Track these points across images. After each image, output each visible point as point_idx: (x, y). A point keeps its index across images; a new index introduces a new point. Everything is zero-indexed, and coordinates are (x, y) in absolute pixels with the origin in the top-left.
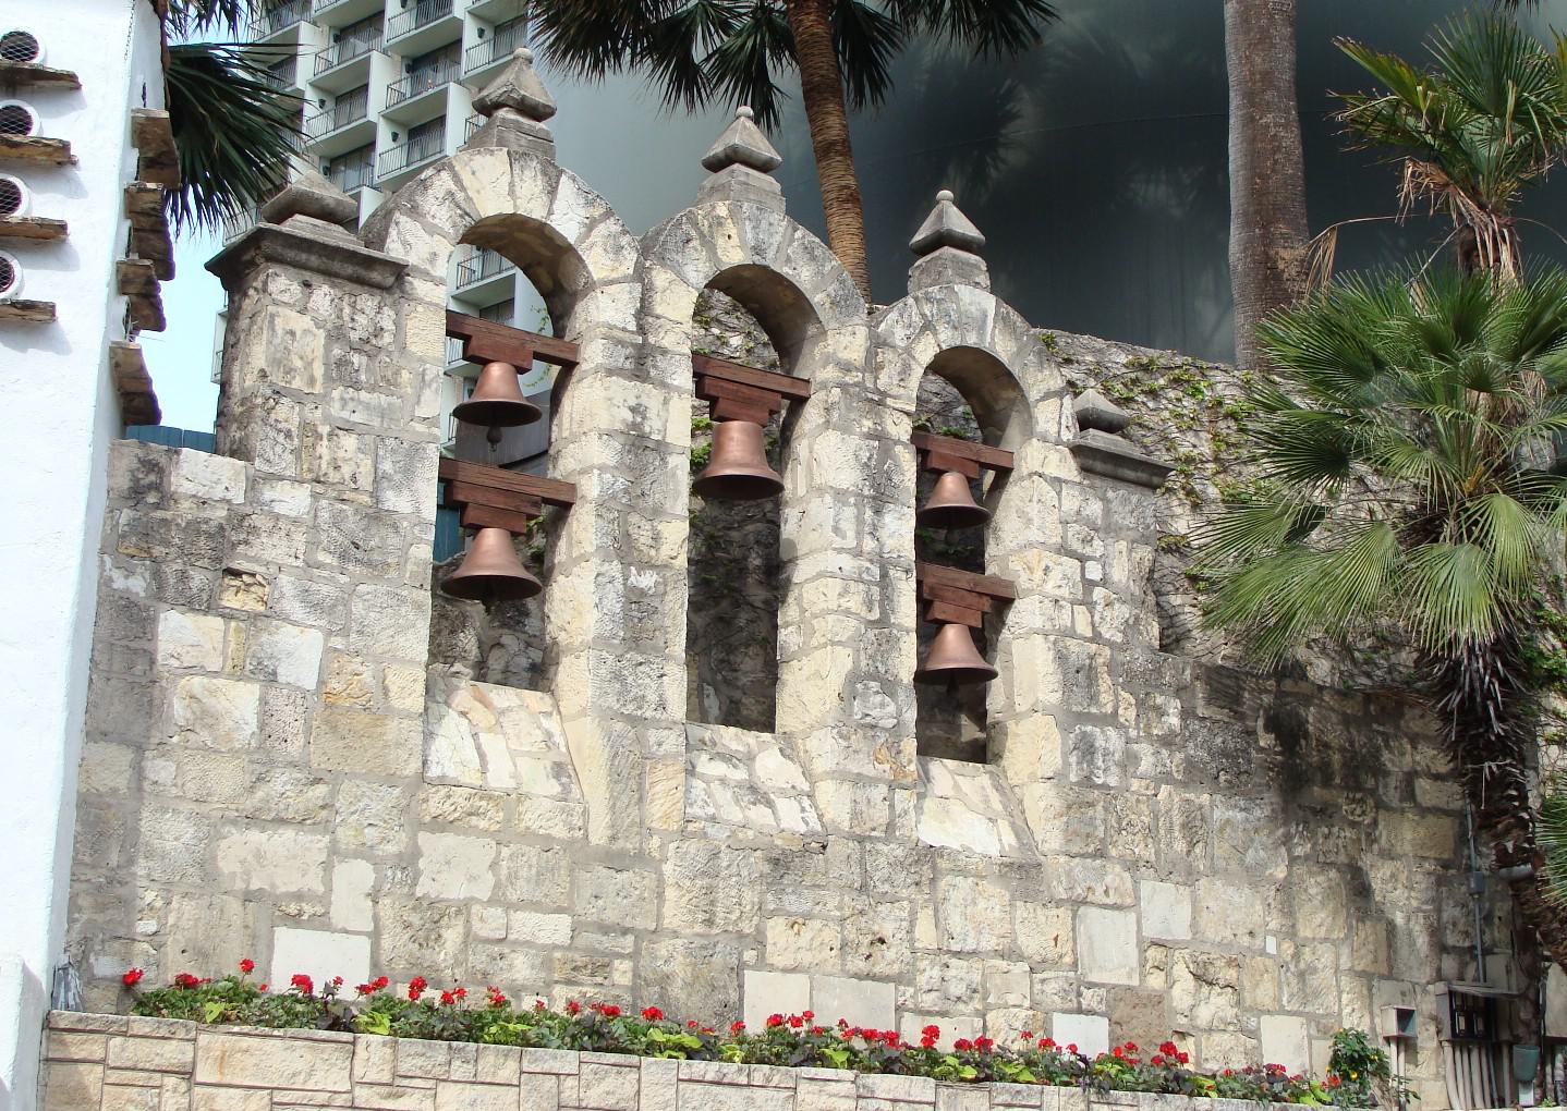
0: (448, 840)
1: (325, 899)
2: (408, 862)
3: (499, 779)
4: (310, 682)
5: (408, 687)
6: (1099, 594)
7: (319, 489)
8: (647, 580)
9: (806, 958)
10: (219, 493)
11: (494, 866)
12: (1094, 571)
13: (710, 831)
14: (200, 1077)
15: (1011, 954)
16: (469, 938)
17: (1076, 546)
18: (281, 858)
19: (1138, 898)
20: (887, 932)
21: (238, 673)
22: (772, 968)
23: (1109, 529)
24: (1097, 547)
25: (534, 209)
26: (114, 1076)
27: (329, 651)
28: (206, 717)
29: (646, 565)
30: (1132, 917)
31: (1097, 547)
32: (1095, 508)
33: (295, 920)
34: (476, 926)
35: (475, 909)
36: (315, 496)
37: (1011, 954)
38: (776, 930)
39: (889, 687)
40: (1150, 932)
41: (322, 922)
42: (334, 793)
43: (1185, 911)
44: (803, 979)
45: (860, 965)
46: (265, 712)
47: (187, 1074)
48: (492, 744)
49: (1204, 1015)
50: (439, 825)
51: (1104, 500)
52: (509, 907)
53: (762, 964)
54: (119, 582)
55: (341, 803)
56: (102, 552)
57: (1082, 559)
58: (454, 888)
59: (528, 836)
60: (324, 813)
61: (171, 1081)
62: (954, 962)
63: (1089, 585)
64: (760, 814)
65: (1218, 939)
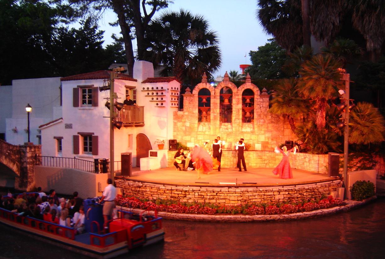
1: (191, 140)
2: (197, 137)
5: (196, 125)
6: (262, 108)
8: (216, 114)
12: (261, 106)
15: (251, 139)
16: (202, 142)
17: (259, 104)
18: (187, 138)
23: (263, 102)
24: (262, 104)
25: (205, 87)
29: (215, 113)
31: (262, 104)
32: (261, 100)
33: (189, 142)
37: (251, 139)
39: (239, 119)
41: (190, 142)
46: (186, 128)
49: (272, 143)
51: (263, 99)
54: (175, 121)
57: (260, 105)
58: (200, 139)
59: (206, 135)
63: (261, 107)
64: (227, 131)
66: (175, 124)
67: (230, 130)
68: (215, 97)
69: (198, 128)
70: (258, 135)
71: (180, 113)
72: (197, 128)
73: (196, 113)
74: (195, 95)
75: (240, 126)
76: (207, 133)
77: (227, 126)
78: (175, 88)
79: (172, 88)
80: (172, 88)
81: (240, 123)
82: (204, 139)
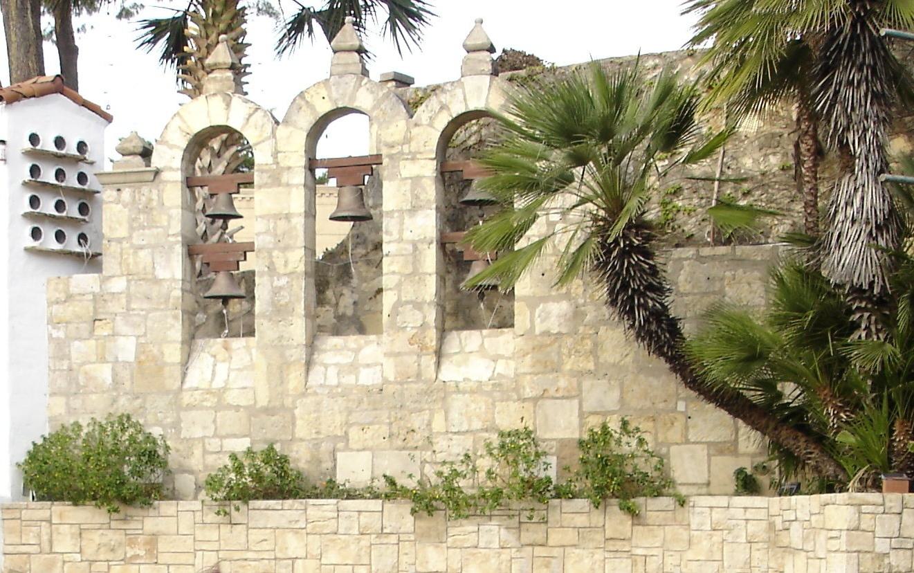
0: (194, 413)
3: (218, 383)
4: (131, 358)
5: (173, 354)
7: (130, 277)
9: (370, 444)
10: (90, 290)
11: (214, 421)
13: (318, 391)
14: (53, 522)
19: (581, 391)
20: (416, 426)
21: (103, 360)
22: (352, 450)
26: (24, 523)
27: (139, 345)
28: (89, 378)
29: (279, 276)
30: (576, 402)
34: (207, 447)
35: (206, 441)
36: (129, 281)
38: (354, 433)
39: (418, 305)
40: (587, 407)
42: (145, 401)
43: (616, 394)
44: (368, 454)
45: (400, 443)
46: (115, 374)
47: (50, 521)
48: (222, 369)
50: (190, 407)
52: (222, 438)
53: (347, 448)
54: (55, 334)
55: (148, 406)
56: (48, 324)
58: (198, 433)
59: (229, 407)
60: (141, 410)
61: (44, 523)
62: (455, 437)
65: (639, 407)
66: (60, 350)
67: (368, 378)
68: (275, 179)
69: (185, 364)
70: (535, 400)
71: (85, 281)
72: (177, 372)
73: (174, 280)
74: (165, 176)
75: (423, 348)
76: (232, 398)
77: (357, 351)
78: (59, 142)
79: (34, 139)
80: (34, 139)
81: (424, 326)
82: (215, 435)
